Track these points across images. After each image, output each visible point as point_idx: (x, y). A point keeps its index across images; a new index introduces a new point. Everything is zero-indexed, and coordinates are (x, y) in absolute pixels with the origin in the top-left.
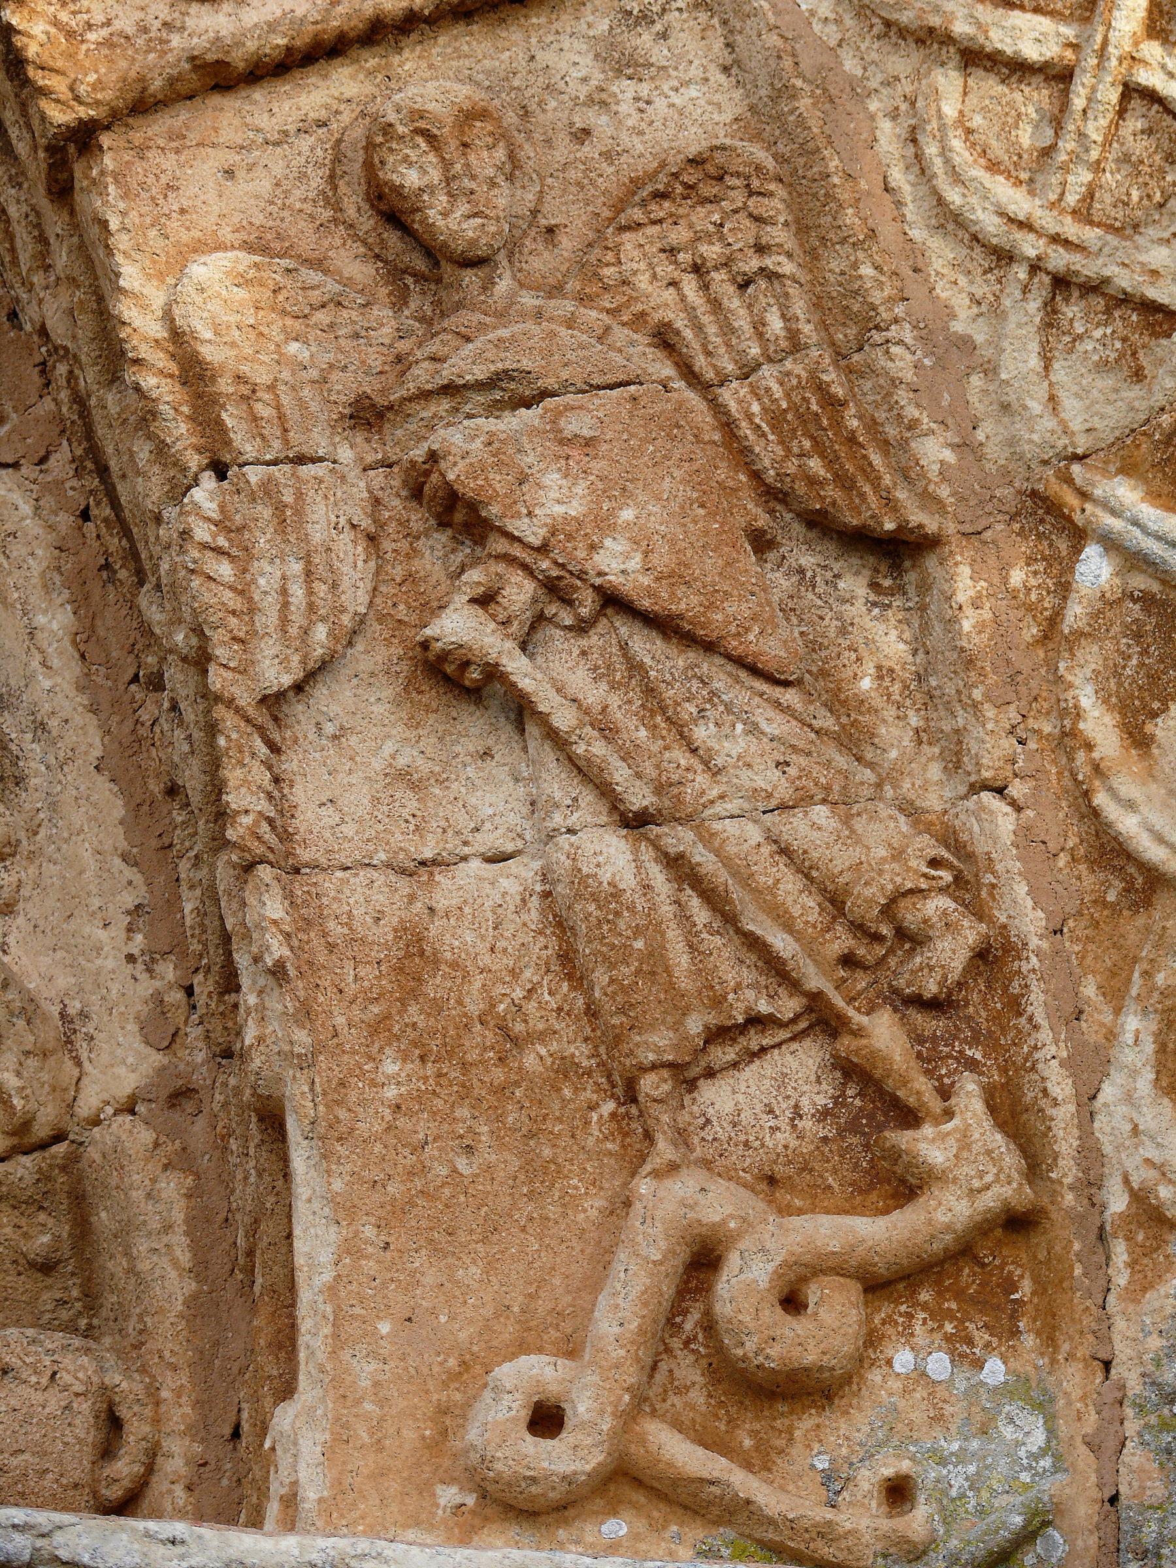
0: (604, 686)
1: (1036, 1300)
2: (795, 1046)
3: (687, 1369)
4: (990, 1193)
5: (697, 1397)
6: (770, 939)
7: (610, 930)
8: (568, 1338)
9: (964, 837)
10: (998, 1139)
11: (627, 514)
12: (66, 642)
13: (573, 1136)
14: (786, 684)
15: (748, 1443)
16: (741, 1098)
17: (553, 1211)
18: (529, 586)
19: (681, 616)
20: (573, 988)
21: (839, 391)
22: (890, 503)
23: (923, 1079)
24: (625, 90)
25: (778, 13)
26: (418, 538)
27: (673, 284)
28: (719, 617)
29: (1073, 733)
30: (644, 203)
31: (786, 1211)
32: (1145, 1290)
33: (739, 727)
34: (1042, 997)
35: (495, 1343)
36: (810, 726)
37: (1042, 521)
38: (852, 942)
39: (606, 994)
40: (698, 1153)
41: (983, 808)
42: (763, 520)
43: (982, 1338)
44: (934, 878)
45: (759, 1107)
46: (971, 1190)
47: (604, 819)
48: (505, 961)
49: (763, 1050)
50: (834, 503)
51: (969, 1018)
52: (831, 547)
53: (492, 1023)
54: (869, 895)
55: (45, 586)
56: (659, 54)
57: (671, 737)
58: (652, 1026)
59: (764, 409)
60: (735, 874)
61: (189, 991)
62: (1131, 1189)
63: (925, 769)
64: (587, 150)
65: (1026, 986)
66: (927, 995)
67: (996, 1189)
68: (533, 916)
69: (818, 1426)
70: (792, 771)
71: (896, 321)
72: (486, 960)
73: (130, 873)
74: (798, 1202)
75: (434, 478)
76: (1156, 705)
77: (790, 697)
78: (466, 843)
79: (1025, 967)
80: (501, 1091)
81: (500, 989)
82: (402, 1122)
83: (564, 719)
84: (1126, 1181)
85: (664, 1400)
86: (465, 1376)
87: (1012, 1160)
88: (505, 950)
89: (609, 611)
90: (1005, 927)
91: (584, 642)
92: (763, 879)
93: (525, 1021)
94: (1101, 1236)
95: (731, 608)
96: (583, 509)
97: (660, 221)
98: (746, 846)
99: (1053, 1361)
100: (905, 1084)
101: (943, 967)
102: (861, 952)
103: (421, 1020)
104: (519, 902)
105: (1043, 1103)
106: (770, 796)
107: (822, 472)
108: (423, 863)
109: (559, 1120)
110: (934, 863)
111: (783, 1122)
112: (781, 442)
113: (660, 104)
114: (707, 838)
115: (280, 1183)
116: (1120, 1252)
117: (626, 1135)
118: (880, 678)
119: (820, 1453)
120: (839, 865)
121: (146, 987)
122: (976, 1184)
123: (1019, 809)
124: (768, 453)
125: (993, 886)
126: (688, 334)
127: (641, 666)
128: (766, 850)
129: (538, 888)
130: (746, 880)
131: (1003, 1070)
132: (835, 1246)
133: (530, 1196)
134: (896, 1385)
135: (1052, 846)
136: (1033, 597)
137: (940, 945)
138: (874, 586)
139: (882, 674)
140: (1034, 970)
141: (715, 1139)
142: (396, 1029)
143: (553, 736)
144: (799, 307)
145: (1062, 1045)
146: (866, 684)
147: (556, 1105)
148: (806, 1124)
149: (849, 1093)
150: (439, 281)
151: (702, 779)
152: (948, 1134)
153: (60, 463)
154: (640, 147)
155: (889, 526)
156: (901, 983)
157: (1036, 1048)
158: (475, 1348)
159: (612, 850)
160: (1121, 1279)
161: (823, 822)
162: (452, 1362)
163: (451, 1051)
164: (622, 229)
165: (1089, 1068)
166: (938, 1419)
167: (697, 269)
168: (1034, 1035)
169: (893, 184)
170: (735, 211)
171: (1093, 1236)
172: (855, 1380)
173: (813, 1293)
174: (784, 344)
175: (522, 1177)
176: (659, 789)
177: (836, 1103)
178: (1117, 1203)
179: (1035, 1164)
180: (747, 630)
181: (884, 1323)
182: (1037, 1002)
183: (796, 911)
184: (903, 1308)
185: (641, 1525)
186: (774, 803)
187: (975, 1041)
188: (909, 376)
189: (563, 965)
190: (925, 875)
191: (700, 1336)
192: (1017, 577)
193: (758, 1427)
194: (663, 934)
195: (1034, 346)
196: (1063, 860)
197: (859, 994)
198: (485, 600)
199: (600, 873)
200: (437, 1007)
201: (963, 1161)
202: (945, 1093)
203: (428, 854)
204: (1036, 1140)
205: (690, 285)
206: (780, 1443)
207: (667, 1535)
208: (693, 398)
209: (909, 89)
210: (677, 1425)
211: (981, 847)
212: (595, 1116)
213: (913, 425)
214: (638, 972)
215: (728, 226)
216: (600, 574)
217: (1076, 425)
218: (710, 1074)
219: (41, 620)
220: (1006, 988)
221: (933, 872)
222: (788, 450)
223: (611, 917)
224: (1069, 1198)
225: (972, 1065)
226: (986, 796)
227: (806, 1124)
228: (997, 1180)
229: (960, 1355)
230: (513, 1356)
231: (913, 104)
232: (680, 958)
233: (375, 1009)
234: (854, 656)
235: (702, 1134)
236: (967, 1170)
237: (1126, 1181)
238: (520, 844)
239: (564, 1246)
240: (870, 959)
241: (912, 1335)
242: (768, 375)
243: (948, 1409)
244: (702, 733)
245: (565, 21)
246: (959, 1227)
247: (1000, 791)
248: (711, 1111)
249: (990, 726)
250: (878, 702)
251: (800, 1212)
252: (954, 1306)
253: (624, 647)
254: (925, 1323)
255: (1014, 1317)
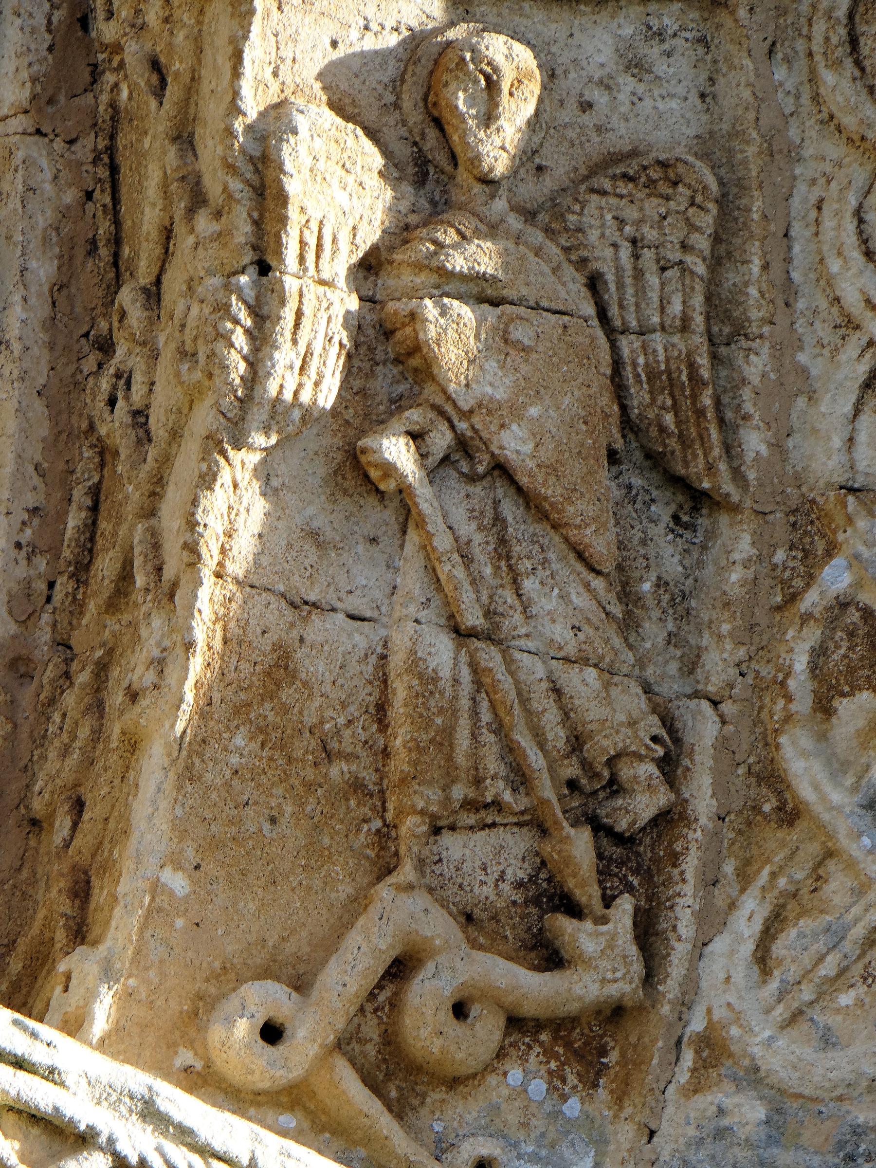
0: (474, 526)
1: (617, 1068)
2: (516, 829)
3: (371, 1030)
4: (616, 985)
5: (371, 1050)
6: (529, 752)
7: (423, 703)
8: (299, 977)
9: (679, 726)
10: (633, 950)
11: (534, 411)
12: (46, 289)
13: (347, 836)
14: (598, 573)
15: (393, 1094)
16: (467, 852)
17: (318, 883)
18: (449, 436)
19: (546, 498)
20: (380, 731)
21: (705, 373)
22: (711, 468)
23: (596, 887)
24: (627, 83)
25: (757, 76)
26: (377, 364)
27: (615, 245)
28: (572, 509)
29: (783, 684)
30: (614, 178)
31: (474, 944)
32: (695, 1092)
33: (556, 591)
34: (696, 862)
35: (250, 962)
36: (604, 608)
37: (812, 523)
38: (579, 772)
39: (405, 747)
40: (427, 880)
41: (700, 712)
42: (619, 445)
43: (572, 1080)
44: (652, 749)
45: (478, 863)
46: (604, 979)
47: (443, 621)
48: (340, 694)
49: (494, 825)
50: (673, 453)
51: (638, 854)
52: (655, 477)
53: (318, 735)
54: (603, 745)
55: (44, 239)
56: (661, 68)
57: (507, 580)
58: (430, 783)
59: (647, 364)
60: (519, 694)
61: (51, 585)
62: (710, 1020)
63: (666, 663)
64: (587, 119)
65: (687, 848)
66: (618, 829)
67: (620, 984)
68: (369, 669)
69: (444, 1100)
70: (581, 636)
71: (761, 336)
72: (327, 688)
73: (36, 480)
74: (482, 940)
75: (408, 330)
76: (846, 689)
77: (598, 583)
78: (339, 599)
79: (691, 835)
80: (310, 786)
81: (330, 713)
82: (236, 782)
83: (443, 542)
84: (709, 1011)
85: (348, 1044)
86: (223, 978)
87: (637, 968)
88: (342, 686)
89: (496, 473)
90: (687, 801)
91: (471, 489)
92: (535, 705)
93: (340, 742)
94: (679, 1042)
95: (582, 505)
96: (505, 396)
97: (621, 197)
98: (532, 678)
99: (616, 1116)
100: (583, 887)
101: (636, 813)
102: (584, 781)
103: (271, 716)
104: (362, 655)
105: (670, 935)
106: (560, 648)
107: (672, 426)
108: (306, 603)
109: (342, 821)
110: (655, 739)
111: (491, 880)
112: (651, 392)
113: (648, 103)
114: (509, 662)
115: (117, 781)
116: (688, 1057)
117: (382, 848)
118: (658, 586)
119: (438, 1119)
120: (590, 716)
121: (21, 571)
122: (609, 975)
123: (724, 722)
124: (639, 396)
125: (688, 769)
126: (612, 287)
127: (504, 521)
128: (545, 685)
129: (379, 650)
130: (524, 701)
131: (649, 899)
132: (503, 983)
133: (305, 868)
134: (505, 1092)
135: (739, 757)
136: (787, 574)
137: (639, 797)
138: (676, 518)
139: (661, 583)
140: (697, 840)
141: (441, 875)
142: (252, 716)
143: (426, 549)
144: (698, 301)
145: (698, 900)
146: (647, 586)
147: (343, 809)
148: (505, 887)
149: (541, 876)
150: (452, 178)
151: (518, 618)
152: (602, 934)
153: (84, 149)
154: (623, 131)
155: (706, 485)
156: (602, 812)
157: (679, 894)
158: (235, 961)
159: (442, 647)
160: (683, 1076)
161: (590, 681)
162: (217, 964)
163: (282, 746)
164: (593, 191)
165: (712, 922)
166: (525, 1125)
167: (634, 241)
168: (681, 885)
169: (792, 233)
170: (678, 212)
171: (673, 1041)
172: (479, 1077)
173: (475, 1010)
174: (678, 323)
175: (303, 852)
176: (489, 614)
177: (530, 880)
178: (697, 1025)
179: (650, 977)
180: (587, 525)
181: (511, 1045)
182: (691, 864)
183: (550, 736)
184: (527, 1040)
185: (306, 1124)
186: (561, 654)
187: (636, 872)
188: (756, 380)
189: (378, 711)
190: (647, 747)
191: (387, 1009)
192: (780, 556)
193: (404, 1085)
194: (457, 719)
195: (853, 398)
196: (741, 770)
197: (572, 809)
198: (416, 436)
199: (429, 659)
200: (285, 710)
201: (601, 955)
202: (608, 901)
203: (312, 597)
204: (657, 959)
205: (625, 253)
206: (415, 1102)
207: (321, 1138)
208: (600, 333)
209: (829, 169)
210: (352, 1062)
211: (689, 738)
212: (365, 827)
213: (746, 417)
214: (432, 741)
215: (669, 220)
216: (501, 448)
217: (861, 466)
218: (452, 828)
219: (33, 264)
220: (671, 844)
221: (652, 745)
222: (653, 400)
223: (427, 694)
224: (666, 1009)
225: (630, 889)
226: (705, 705)
227: (505, 887)
228: (623, 978)
229: (554, 1087)
230: (259, 977)
231: (829, 182)
232: (462, 740)
233: (243, 695)
234: (645, 564)
235: (434, 867)
236: (604, 964)
237: (709, 1011)
238: (376, 614)
239: (316, 912)
240: (588, 789)
241: (527, 1061)
242: (658, 341)
243: (534, 1122)
244: (529, 585)
245: (603, 17)
246: (587, 1000)
247: (715, 704)
248: (444, 854)
249: (725, 655)
250: (650, 602)
251: (481, 948)
252: (561, 1051)
253: (496, 503)
254: (538, 1056)
255: (598, 1074)
